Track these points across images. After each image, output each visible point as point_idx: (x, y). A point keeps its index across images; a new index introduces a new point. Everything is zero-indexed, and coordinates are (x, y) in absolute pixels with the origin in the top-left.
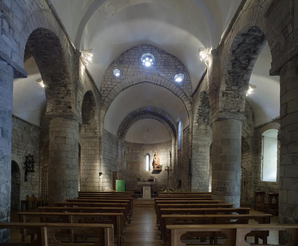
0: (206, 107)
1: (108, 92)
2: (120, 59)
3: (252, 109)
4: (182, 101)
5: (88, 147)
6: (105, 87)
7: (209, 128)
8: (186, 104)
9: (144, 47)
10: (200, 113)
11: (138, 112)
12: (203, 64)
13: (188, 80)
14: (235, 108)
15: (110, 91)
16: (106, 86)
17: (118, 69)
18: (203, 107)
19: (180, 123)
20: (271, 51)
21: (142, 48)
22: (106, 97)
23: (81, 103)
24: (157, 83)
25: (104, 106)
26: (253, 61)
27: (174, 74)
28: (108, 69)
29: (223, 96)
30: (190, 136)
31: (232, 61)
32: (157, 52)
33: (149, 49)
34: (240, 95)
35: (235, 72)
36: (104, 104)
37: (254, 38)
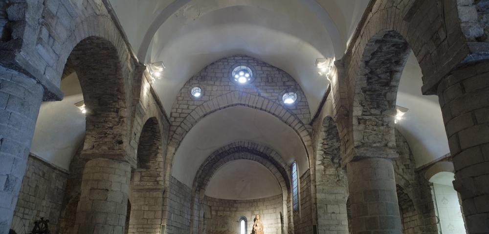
0: (335, 140)
2: (202, 74)
3: (406, 142)
4: (297, 131)
7: (341, 173)
8: (302, 136)
9: (236, 58)
11: (227, 148)
12: (324, 80)
13: (302, 102)
14: (379, 142)
17: (199, 87)
19: (295, 165)
21: (234, 59)
22: (178, 126)
24: (257, 106)
25: (173, 140)
26: (397, 75)
29: (359, 123)
30: (312, 187)
31: (367, 74)
32: (256, 64)
33: (243, 61)
34: (386, 122)
35: (373, 90)
36: (174, 136)
37: (393, 46)
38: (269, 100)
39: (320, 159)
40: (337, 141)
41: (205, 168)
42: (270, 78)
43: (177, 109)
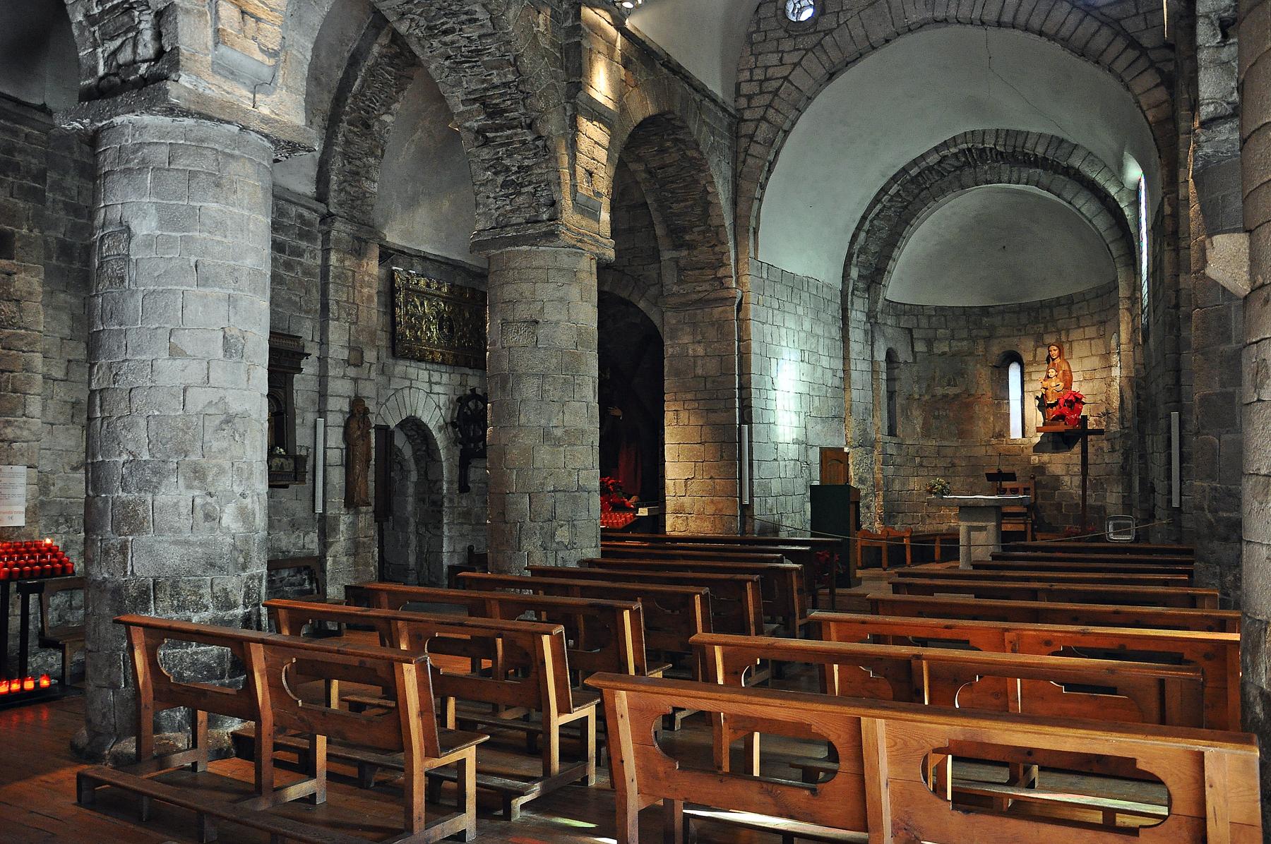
1: (766, 99)
5: (691, 347)
6: (755, 78)
15: (776, 93)
16: (759, 74)
22: (759, 120)
24: (986, 18)
43: (751, 70)
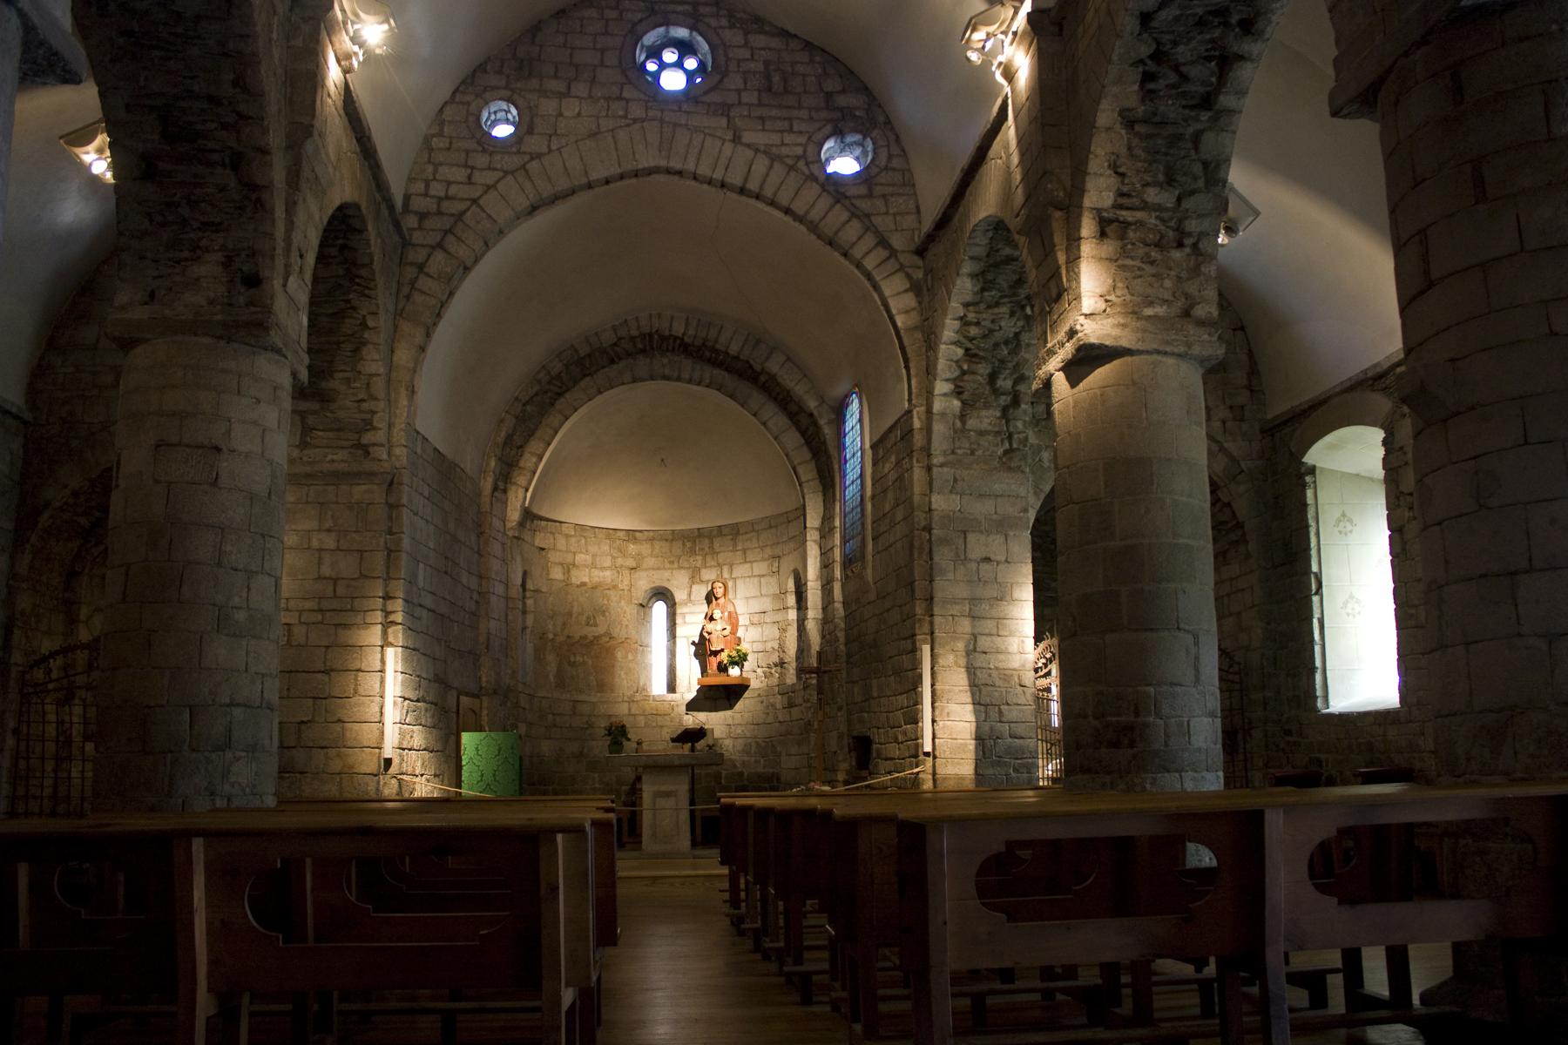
0: (1004, 309)
1: (446, 223)
4: (869, 276)
7: (1020, 425)
8: (887, 292)
10: (971, 339)
11: (608, 338)
12: (977, 83)
13: (894, 169)
15: (459, 216)
16: (437, 189)
17: (509, 100)
18: (983, 306)
20: (1330, 11)
22: (433, 248)
23: (311, 259)
24: (728, 180)
27: (819, 136)
28: (452, 100)
30: (918, 474)
31: (1142, 61)
32: (724, 22)
34: (1190, 234)
36: (419, 284)
38: (774, 159)
39: (948, 375)
40: (1012, 314)
41: (528, 408)
42: (776, 78)
